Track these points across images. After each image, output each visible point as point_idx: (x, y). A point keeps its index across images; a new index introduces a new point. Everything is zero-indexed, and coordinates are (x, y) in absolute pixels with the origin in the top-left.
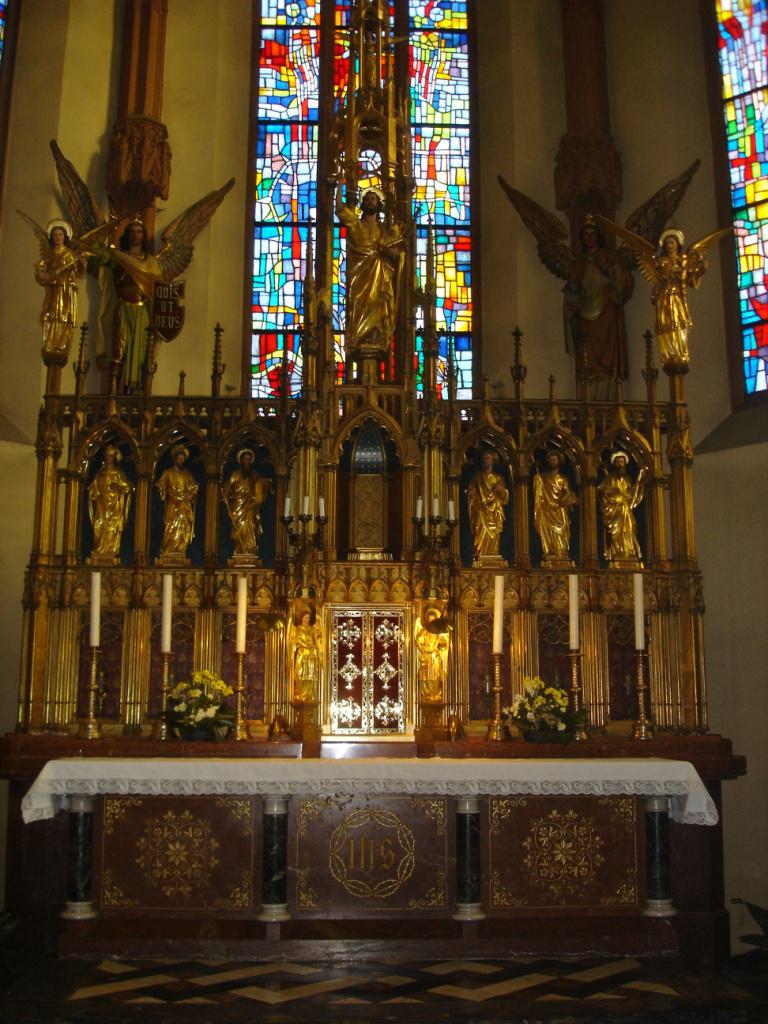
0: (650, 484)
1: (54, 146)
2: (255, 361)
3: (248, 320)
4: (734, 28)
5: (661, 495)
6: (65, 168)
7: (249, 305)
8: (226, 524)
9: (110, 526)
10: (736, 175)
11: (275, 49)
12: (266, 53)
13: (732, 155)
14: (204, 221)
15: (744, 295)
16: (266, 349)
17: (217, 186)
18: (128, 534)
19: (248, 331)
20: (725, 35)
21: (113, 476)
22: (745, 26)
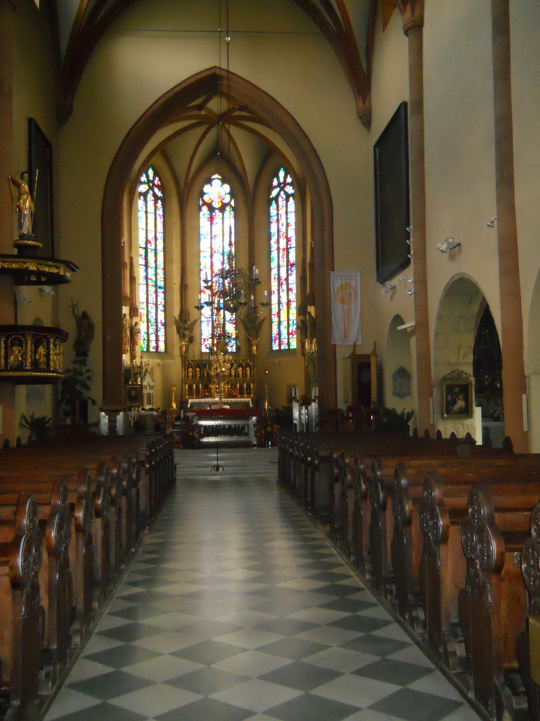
0: (251, 368)
1: (174, 317)
2: (203, 343)
3: (201, 337)
4: (274, 292)
5: (252, 369)
6: (176, 320)
7: (201, 335)
8: (203, 375)
9: (190, 375)
10: (273, 316)
11: (204, 291)
12: (202, 291)
13: (272, 313)
14: (195, 324)
15: (273, 335)
16: (204, 340)
17: (197, 319)
18: (192, 375)
19: (201, 339)
20: (273, 293)
21: (191, 369)
22: (275, 293)
